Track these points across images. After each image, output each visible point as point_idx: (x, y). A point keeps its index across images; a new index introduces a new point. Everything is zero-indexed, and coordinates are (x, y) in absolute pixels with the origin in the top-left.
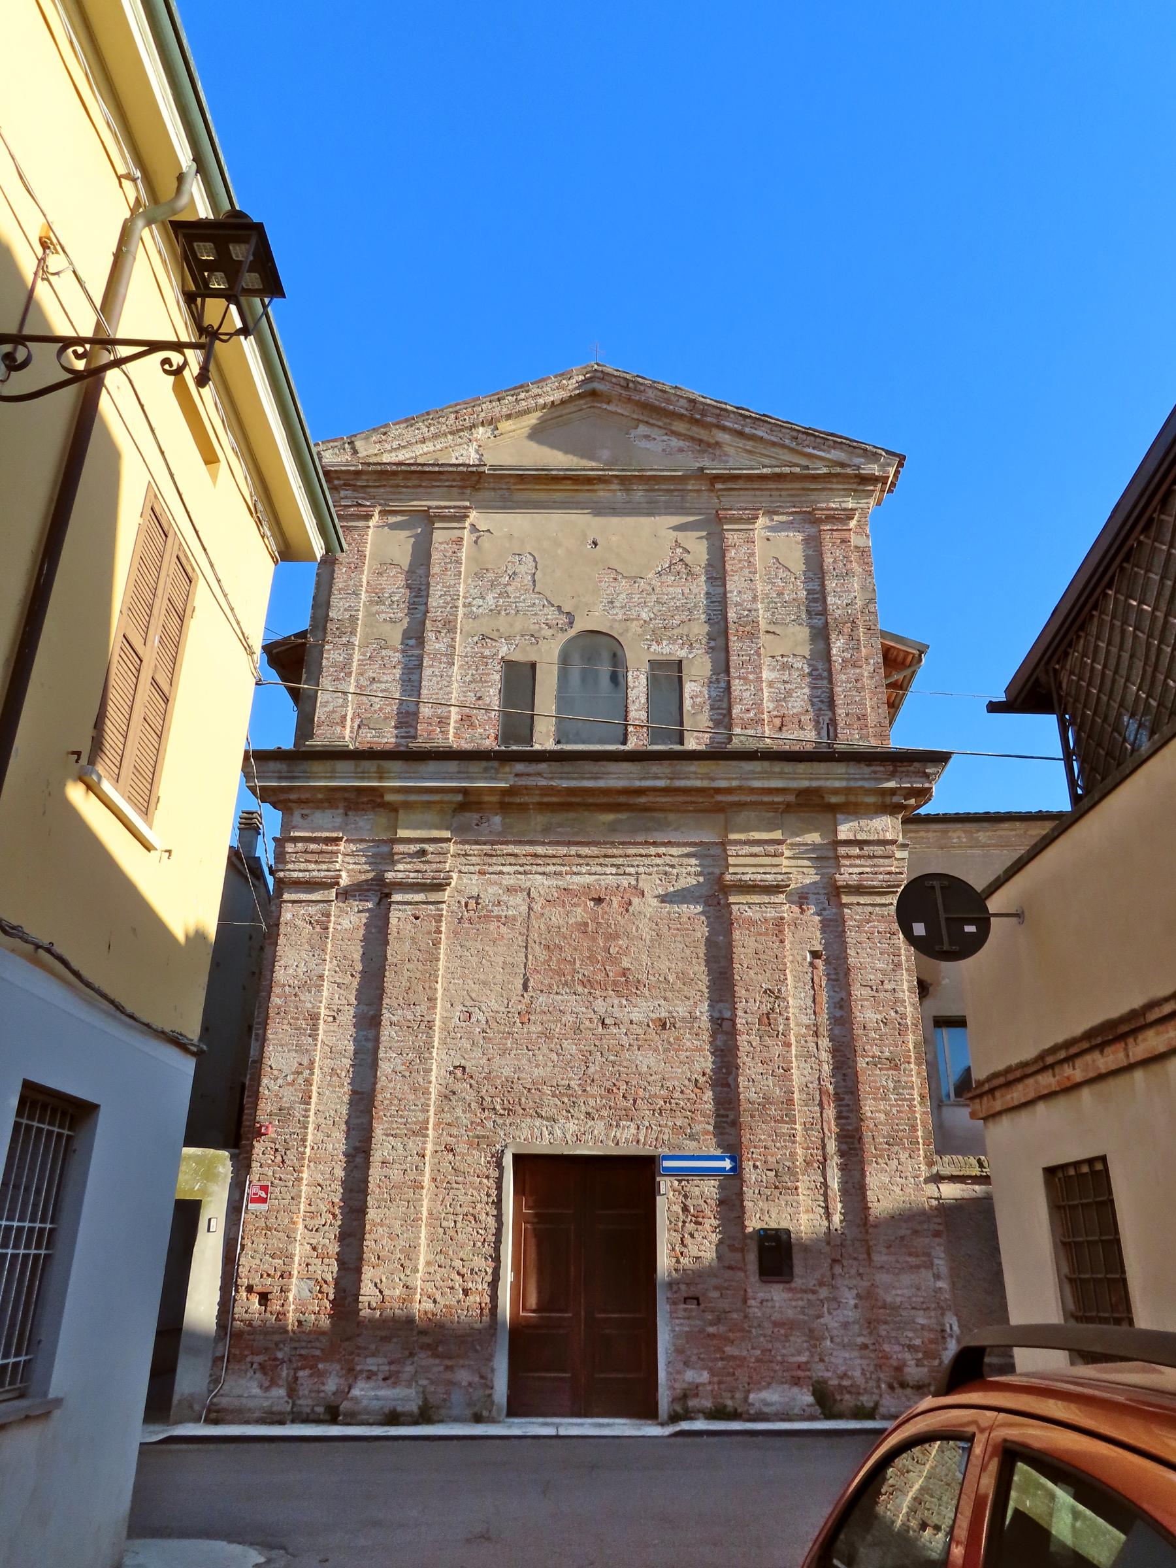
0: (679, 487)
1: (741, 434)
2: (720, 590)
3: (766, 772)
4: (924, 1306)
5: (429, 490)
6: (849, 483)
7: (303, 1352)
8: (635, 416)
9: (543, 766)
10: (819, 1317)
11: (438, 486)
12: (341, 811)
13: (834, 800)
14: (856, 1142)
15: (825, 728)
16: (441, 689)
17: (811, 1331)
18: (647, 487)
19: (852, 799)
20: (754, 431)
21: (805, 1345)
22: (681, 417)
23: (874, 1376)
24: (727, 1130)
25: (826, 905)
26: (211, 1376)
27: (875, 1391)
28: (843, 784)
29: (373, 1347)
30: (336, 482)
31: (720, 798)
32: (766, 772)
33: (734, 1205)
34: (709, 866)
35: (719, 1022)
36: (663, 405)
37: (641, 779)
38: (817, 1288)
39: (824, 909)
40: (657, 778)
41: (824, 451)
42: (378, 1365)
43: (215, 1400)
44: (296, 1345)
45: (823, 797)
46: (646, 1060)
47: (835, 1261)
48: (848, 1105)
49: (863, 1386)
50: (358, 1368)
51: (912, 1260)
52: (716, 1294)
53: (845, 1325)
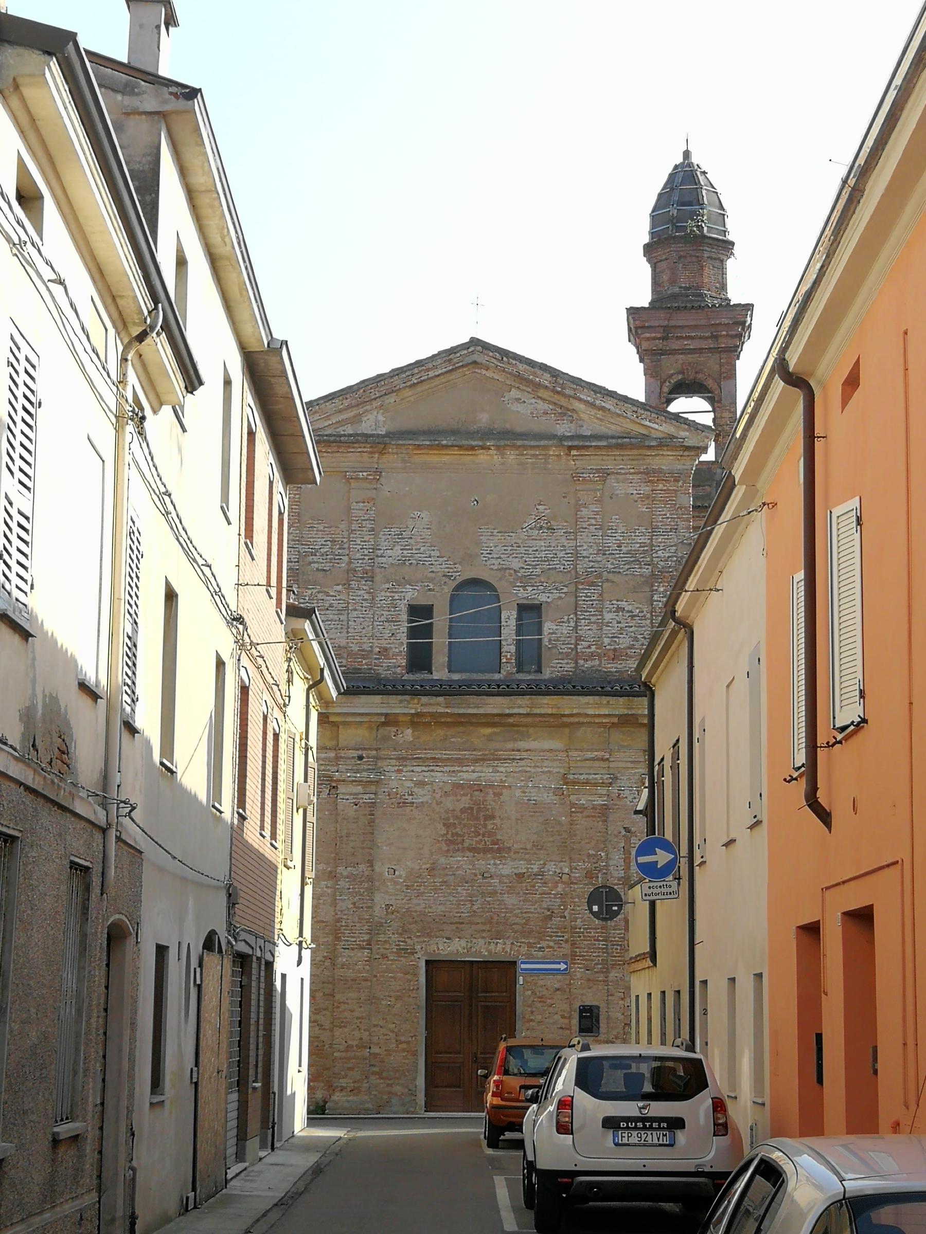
1: (593, 405)
2: (573, 543)
5: (345, 455)
8: (508, 382)
9: (441, 699)
20: (603, 404)
24: (563, 946)
29: (343, 1073)
34: (557, 767)
36: (531, 377)
37: (509, 708)
39: (635, 798)
40: (520, 707)
45: (637, 719)
46: (511, 900)
50: (335, 1085)
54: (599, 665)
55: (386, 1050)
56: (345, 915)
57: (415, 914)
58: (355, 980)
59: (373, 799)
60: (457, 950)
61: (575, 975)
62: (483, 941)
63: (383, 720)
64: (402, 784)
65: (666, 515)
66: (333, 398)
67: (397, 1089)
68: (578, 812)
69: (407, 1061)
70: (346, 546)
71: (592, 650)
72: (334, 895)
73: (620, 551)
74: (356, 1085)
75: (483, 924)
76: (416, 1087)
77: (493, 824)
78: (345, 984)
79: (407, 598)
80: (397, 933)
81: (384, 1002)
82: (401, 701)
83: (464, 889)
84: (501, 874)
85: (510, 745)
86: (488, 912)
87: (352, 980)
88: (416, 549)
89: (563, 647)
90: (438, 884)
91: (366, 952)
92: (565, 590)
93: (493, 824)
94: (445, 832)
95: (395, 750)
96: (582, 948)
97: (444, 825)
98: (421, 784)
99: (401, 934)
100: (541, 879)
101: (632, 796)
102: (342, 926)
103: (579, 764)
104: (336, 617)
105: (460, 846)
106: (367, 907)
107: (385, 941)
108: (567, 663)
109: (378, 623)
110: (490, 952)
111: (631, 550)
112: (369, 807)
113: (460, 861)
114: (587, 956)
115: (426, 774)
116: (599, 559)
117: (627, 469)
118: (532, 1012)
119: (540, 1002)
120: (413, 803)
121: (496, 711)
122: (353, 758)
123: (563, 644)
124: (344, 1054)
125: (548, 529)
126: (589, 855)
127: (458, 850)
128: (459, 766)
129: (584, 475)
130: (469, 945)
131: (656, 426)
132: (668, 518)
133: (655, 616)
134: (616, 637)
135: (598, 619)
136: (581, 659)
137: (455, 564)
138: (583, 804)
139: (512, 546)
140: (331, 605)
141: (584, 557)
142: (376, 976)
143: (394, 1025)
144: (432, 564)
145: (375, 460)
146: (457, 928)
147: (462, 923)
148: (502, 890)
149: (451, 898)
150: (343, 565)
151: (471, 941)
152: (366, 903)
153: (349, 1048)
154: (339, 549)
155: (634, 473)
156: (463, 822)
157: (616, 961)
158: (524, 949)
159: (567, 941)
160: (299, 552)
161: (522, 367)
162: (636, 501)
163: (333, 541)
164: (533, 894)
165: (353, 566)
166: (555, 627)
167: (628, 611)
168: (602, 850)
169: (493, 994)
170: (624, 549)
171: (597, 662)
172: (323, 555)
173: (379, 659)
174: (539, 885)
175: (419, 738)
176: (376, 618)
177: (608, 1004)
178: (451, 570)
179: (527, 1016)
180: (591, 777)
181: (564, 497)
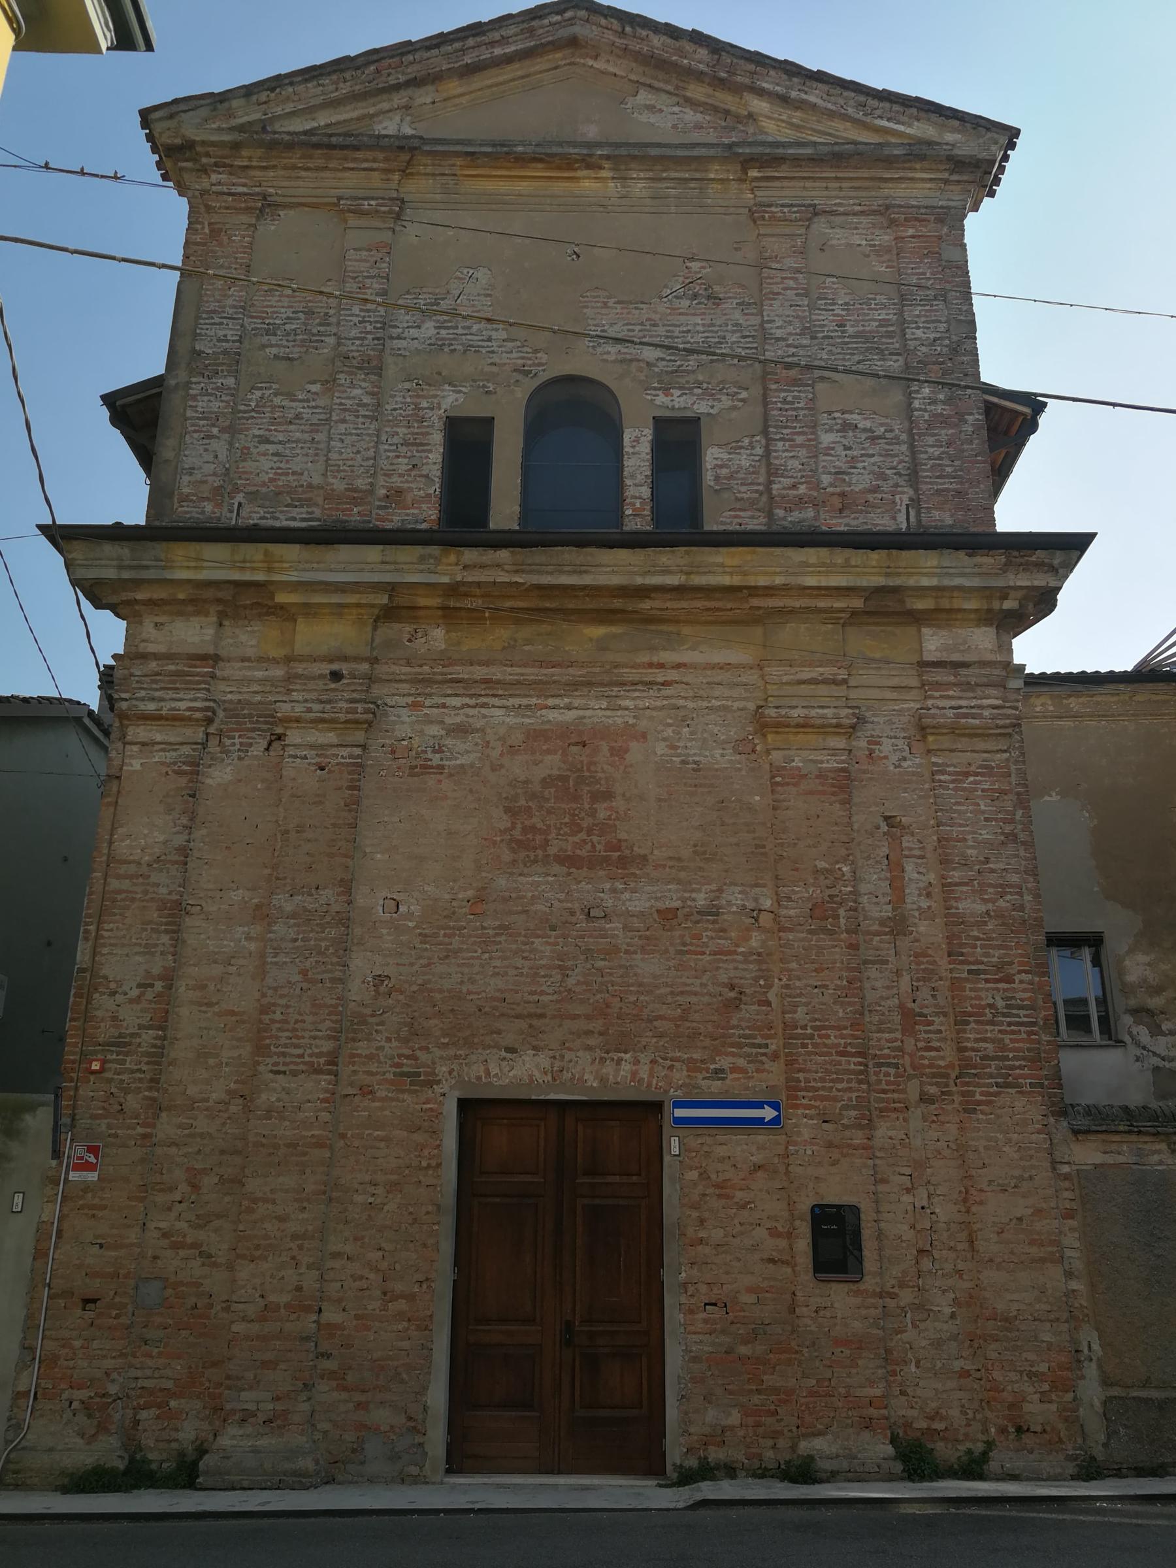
0: (698, 175)
1: (784, 100)
2: (756, 320)
3: (823, 565)
4: (1052, 1317)
5: (340, 175)
6: (938, 170)
7: (146, 1383)
8: (633, 77)
9: (504, 555)
10: (898, 1332)
11: (353, 169)
12: (213, 619)
13: (920, 605)
14: (952, 1082)
15: (904, 511)
16: (358, 452)
17: (888, 1351)
18: (651, 175)
19: (945, 604)
20: (804, 96)
21: (880, 1372)
22: (699, 76)
23: (979, 1416)
24: (766, 1066)
25: (906, 754)
26: (9, 1419)
27: (980, 1436)
28: (934, 582)
29: (250, 1375)
30: (204, 160)
31: (755, 602)
32: (823, 565)
33: (776, 1172)
35: (755, 914)
36: (674, 58)
38: (896, 1290)
39: (905, 759)
40: (666, 571)
41: (903, 124)
42: (258, 1402)
43: (12, 1456)
44: (139, 1373)
45: (904, 602)
46: (649, 967)
47: (921, 1251)
48: (940, 1032)
49: (962, 1431)
50: (228, 1407)
52: (750, 1299)
53: (938, 1344)
54: (816, 518)
55: (357, 1317)
56: (282, 996)
57: (438, 996)
58: (295, 1146)
59: (359, 757)
60: (531, 1076)
61: (799, 1133)
62: (587, 1056)
63: (384, 599)
64: (422, 731)
65: (924, 274)
66: (321, 75)
67: (381, 1417)
68: (788, 784)
69: (405, 1344)
70: (333, 320)
71: (801, 491)
72: (262, 956)
73: (843, 332)
74: (279, 1407)
75: (588, 1017)
76: (425, 1409)
77: (611, 808)
78: (270, 1154)
79: (444, 406)
80: (398, 1039)
81: (359, 1198)
82: (422, 559)
83: (547, 943)
84: (628, 911)
85: (644, 658)
86: (601, 992)
87: (288, 1146)
88: (463, 328)
89: (743, 489)
90: (491, 932)
91: (324, 1080)
92: (744, 395)
93: (611, 808)
94: (509, 825)
95: (409, 664)
96: (809, 1071)
97: (507, 810)
98: (461, 730)
99: (406, 1041)
100: (714, 922)
101: (898, 755)
102: (273, 1021)
103: (789, 690)
104: (307, 436)
105: (540, 852)
106: (332, 980)
107: (370, 1057)
108: (752, 517)
109: (386, 447)
110: (603, 1080)
111: (863, 331)
112: (349, 773)
113: (538, 884)
114: (823, 1088)
115: (471, 711)
116: (805, 342)
117: (849, 205)
118: (702, 1221)
119: (719, 1196)
120: (442, 767)
121: (616, 580)
122: (322, 676)
123: (742, 484)
124: (255, 1328)
125: (709, 298)
126: (817, 872)
127: (535, 861)
128: (539, 697)
129: (773, 209)
130: (557, 1065)
131: (901, 128)
132: (929, 279)
133: (918, 434)
134: (843, 473)
135: (810, 440)
136: (780, 508)
137: (536, 351)
138: (799, 768)
139: (642, 324)
140: (298, 416)
141: (778, 339)
142: (343, 1136)
143: (380, 1253)
144: (493, 352)
145: (394, 185)
146: (531, 1026)
147: (542, 1016)
148: (628, 944)
149: (519, 962)
150: (326, 351)
151: (563, 1057)
152: (331, 971)
153: (269, 1310)
154: (320, 325)
155: (862, 213)
156: (548, 805)
157: (887, 1101)
158: (680, 1075)
159: (775, 1057)
160: (242, 326)
161: (657, 41)
162: (868, 256)
163: (310, 313)
164: (696, 953)
165: (343, 349)
166: (726, 456)
167: (865, 430)
168: (845, 860)
169: (610, 1179)
170: (850, 330)
171: (810, 513)
172: (288, 334)
173: (386, 507)
174: (709, 933)
175: (459, 644)
176: (384, 438)
177: (877, 1202)
178: (530, 362)
179: (690, 1232)
180: (813, 713)
181: (736, 249)
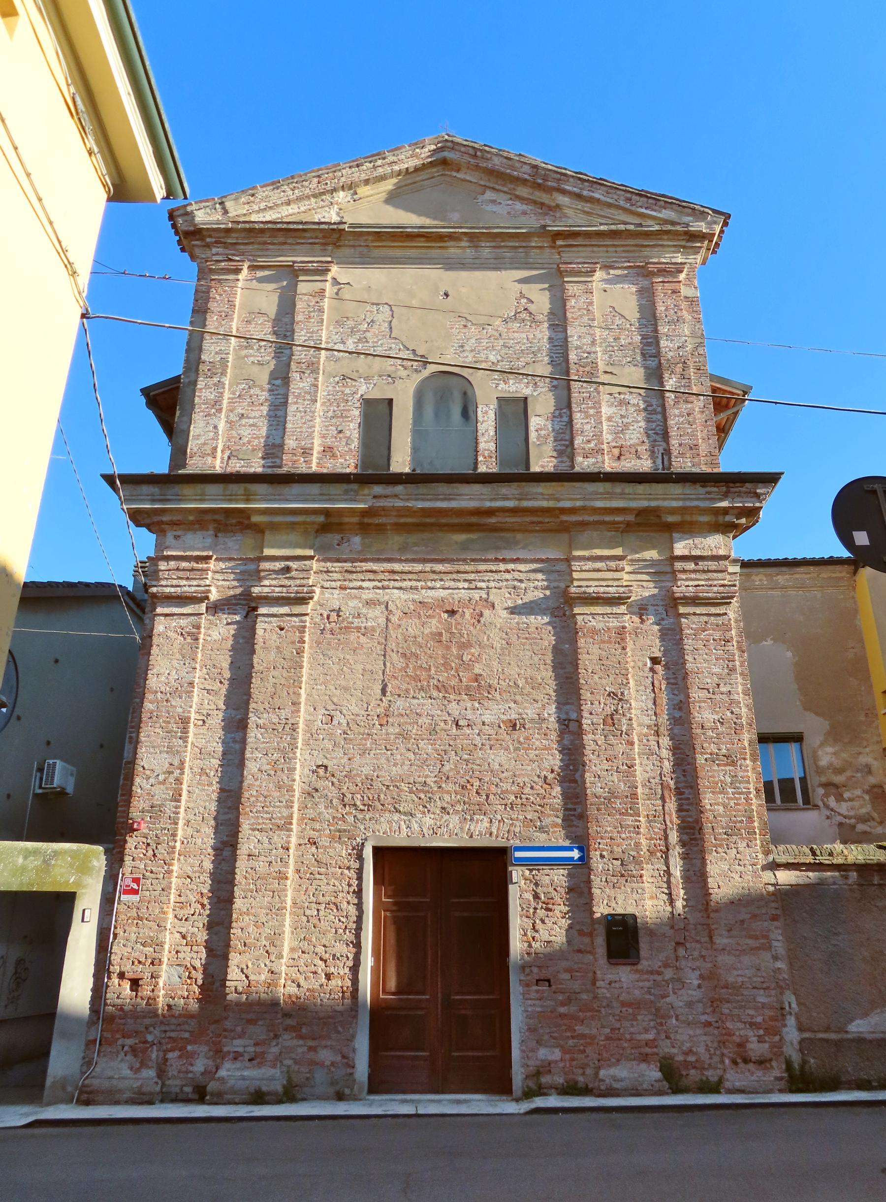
0: (524, 244)
1: (579, 196)
2: (562, 336)
3: (608, 493)
4: (765, 986)
6: (679, 240)
7: (173, 1034)
8: (482, 183)
9: (399, 489)
10: (664, 996)
11: (302, 243)
12: (211, 532)
13: (671, 519)
14: (697, 832)
15: (660, 457)
16: (305, 423)
17: (658, 1010)
18: (493, 244)
19: (688, 518)
21: (652, 1024)
22: (524, 182)
23: (718, 1052)
24: (575, 823)
25: (664, 616)
26: (84, 1058)
27: (719, 1066)
28: (680, 504)
29: (239, 1029)
30: (208, 240)
31: (565, 518)
32: (608, 493)
33: (582, 893)
34: (555, 581)
35: (566, 723)
36: (508, 171)
37: (491, 500)
38: (662, 969)
39: (663, 619)
40: (506, 499)
41: (655, 211)
42: (245, 1047)
43: (87, 1082)
44: (167, 1028)
45: (659, 517)
46: (498, 758)
47: (678, 944)
48: (688, 799)
49: (708, 1062)
50: (225, 1049)
51: (751, 942)
52: (567, 976)
53: (690, 1004)
94: (404, 665)
121: (473, 504)
